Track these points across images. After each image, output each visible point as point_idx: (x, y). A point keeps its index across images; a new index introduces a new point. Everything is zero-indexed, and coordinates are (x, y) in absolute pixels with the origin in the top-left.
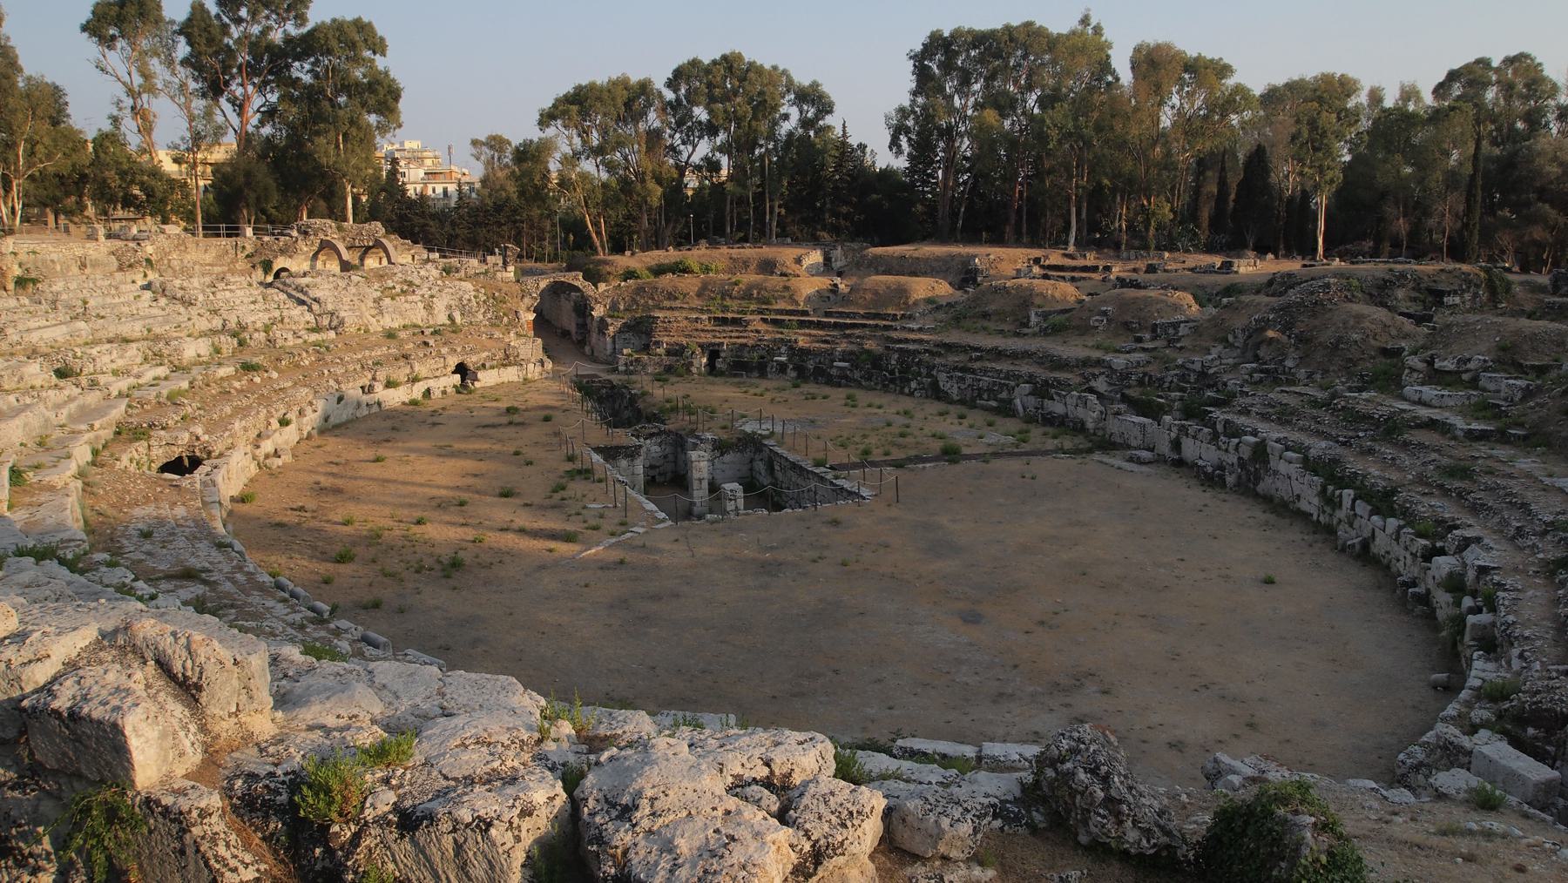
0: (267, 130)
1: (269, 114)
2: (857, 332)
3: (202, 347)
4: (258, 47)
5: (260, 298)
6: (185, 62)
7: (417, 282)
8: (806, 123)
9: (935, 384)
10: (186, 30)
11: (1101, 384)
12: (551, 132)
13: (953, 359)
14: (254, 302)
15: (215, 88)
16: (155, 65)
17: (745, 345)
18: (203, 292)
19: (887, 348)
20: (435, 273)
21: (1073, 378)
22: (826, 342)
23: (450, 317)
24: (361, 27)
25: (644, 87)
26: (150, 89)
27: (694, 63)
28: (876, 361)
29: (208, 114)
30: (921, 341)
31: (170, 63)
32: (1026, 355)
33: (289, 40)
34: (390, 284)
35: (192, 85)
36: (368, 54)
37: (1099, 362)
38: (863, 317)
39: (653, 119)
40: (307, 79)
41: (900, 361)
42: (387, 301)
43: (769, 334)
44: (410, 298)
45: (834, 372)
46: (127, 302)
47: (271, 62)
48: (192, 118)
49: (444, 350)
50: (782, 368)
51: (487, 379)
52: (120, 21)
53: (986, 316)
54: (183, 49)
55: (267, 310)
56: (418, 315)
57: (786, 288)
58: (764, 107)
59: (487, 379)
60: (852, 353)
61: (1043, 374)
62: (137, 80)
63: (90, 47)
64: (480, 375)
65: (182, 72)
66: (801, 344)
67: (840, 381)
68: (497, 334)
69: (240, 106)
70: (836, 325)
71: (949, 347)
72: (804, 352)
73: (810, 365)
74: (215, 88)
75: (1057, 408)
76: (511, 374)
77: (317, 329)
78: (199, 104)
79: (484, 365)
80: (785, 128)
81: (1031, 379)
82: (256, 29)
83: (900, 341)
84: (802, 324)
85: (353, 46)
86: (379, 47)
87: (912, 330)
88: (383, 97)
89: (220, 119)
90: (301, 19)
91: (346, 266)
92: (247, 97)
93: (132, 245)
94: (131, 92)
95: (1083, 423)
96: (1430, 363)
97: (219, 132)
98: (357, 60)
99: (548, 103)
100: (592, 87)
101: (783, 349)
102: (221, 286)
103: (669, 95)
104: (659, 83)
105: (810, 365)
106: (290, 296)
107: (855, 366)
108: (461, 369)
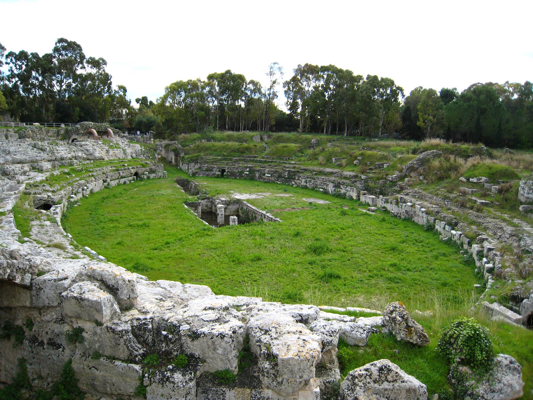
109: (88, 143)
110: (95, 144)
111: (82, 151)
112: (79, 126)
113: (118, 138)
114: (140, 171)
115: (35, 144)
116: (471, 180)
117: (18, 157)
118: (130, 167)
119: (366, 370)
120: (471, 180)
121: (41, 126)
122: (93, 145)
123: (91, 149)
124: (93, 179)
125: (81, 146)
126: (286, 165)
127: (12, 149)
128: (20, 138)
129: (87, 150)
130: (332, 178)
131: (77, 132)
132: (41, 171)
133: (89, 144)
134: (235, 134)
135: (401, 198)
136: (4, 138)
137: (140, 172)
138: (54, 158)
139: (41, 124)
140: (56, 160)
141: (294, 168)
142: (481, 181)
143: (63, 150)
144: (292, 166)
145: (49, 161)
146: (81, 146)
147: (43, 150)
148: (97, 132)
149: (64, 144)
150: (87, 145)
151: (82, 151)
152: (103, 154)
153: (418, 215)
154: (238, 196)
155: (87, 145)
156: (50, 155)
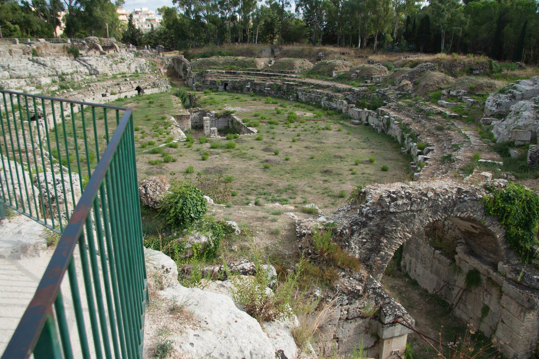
2: (275, 78)
3: (48, 81)
5: (70, 64)
7: (126, 58)
9: (297, 97)
11: (350, 97)
14: (68, 66)
17: (237, 81)
18: (51, 62)
19: (284, 83)
20: (132, 55)
21: (340, 95)
22: (263, 81)
23: (136, 71)
28: (279, 88)
30: (294, 81)
34: (116, 59)
37: (350, 90)
38: (278, 72)
41: (287, 88)
42: (114, 66)
44: (123, 64)
45: (265, 91)
46: (23, 65)
49: (132, 82)
50: (249, 89)
51: (147, 92)
55: (72, 68)
56: (126, 70)
57: (253, 62)
59: (147, 92)
60: (272, 85)
64: (145, 91)
66: (255, 81)
68: (151, 76)
70: (268, 75)
73: (258, 89)
75: (334, 105)
76: (156, 90)
77: (91, 74)
79: (146, 88)
81: (327, 95)
83: (288, 81)
87: (293, 77)
91: (102, 53)
93: (28, 46)
95: (341, 110)
101: (249, 83)
102: (57, 59)
105: (258, 89)
106: (81, 63)
107: (272, 89)
108: (138, 89)
109: (91, 58)
110: (99, 59)
111: (86, 66)
112: (84, 42)
114: (143, 85)
115: (37, 60)
116: (451, 93)
117: (18, 73)
118: (132, 82)
120: (451, 93)
121: (47, 42)
122: (97, 60)
124: (92, 93)
125: (84, 61)
126: (286, 79)
127: (11, 66)
128: (24, 54)
129: (90, 65)
130: (326, 91)
134: (239, 46)
135: (382, 111)
136: (8, 54)
137: (142, 86)
138: (55, 73)
139: (46, 40)
140: (57, 75)
141: (294, 81)
142: (460, 94)
143: (65, 64)
144: (293, 79)
145: (49, 76)
148: (103, 47)
149: (67, 59)
150: (90, 60)
151: (86, 66)
152: (107, 70)
153: (392, 128)
154: (230, 109)
155: (90, 60)
156: (52, 70)
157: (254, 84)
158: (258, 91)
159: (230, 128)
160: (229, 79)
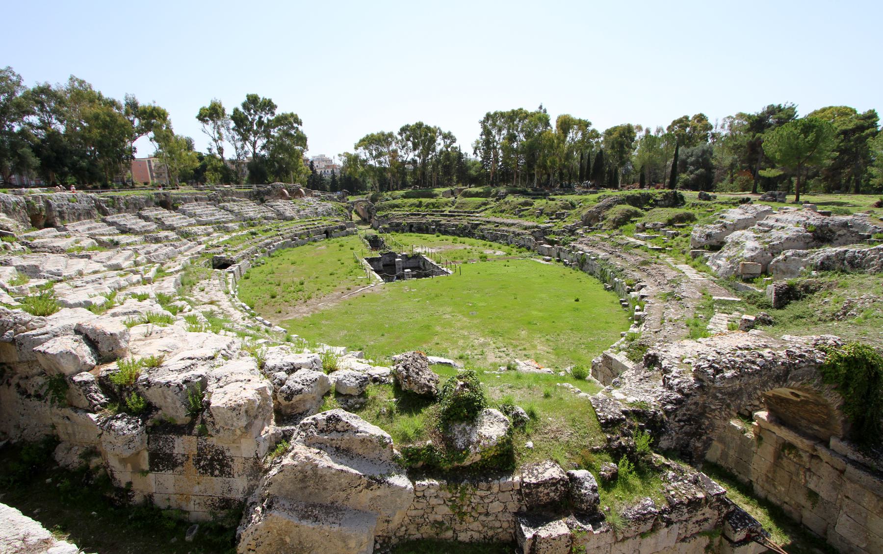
0: (263, 153)
1: (263, 147)
4: (260, 123)
6: (233, 129)
8: (447, 147)
10: (233, 118)
12: (358, 151)
13: (488, 226)
15: (245, 139)
16: (223, 131)
24: (292, 115)
25: (390, 135)
26: (221, 138)
27: (408, 126)
28: (465, 228)
29: (243, 148)
31: (228, 129)
32: (513, 224)
33: (269, 120)
35: (237, 137)
36: (295, 125)
39: (393, 146)
40: (276, 135)
43: (430, 219)
47: (265, 128)
48: (237, 148)
50: (434, 230)
52: (211, 116)
53: (502, 212)
54: (232, 124)
58: (433, 140)
61: (518, 230)
62: (217, 136)
63: (200, 124)
65: (235, 133)
67: (453, 234)
69: (254, 145)
71: (488, 222)
72: (441, 225)
74: (245, 139)
78: (239, 144)
80: (438, 149)
81: (514, 233)
82: (257, 117)
84: (442, 215)
85: (291, 123)
86: (300, 123)
88: (302, 140)
89: (246, 149)
90: (273, 114)
92: (255, 142)
94: (215, 140)
96: (644, 225)
97: (246, 153)
98: (293, 128)
99: (357, 141)
100: (372, 135)
103: (399, 138)
104: (396, 134)
113: (310, 198)
119: (314, 419)
123: (281, 210)
131: (269, 193)
132: (227, 231)
133: (281, 204)
146: (272, 207)
147: (231, 212)
154: (418, 250)
157: (438, 224)
158: (442, 230)
159: (420, 268)
160: (414, 220)
